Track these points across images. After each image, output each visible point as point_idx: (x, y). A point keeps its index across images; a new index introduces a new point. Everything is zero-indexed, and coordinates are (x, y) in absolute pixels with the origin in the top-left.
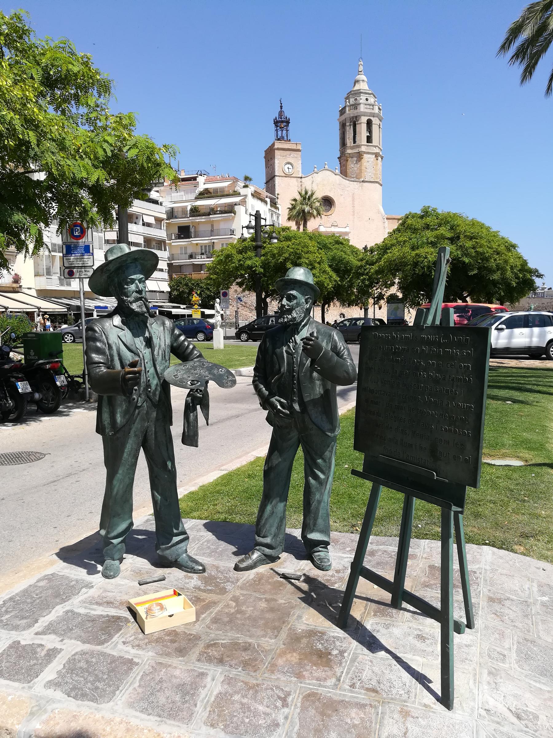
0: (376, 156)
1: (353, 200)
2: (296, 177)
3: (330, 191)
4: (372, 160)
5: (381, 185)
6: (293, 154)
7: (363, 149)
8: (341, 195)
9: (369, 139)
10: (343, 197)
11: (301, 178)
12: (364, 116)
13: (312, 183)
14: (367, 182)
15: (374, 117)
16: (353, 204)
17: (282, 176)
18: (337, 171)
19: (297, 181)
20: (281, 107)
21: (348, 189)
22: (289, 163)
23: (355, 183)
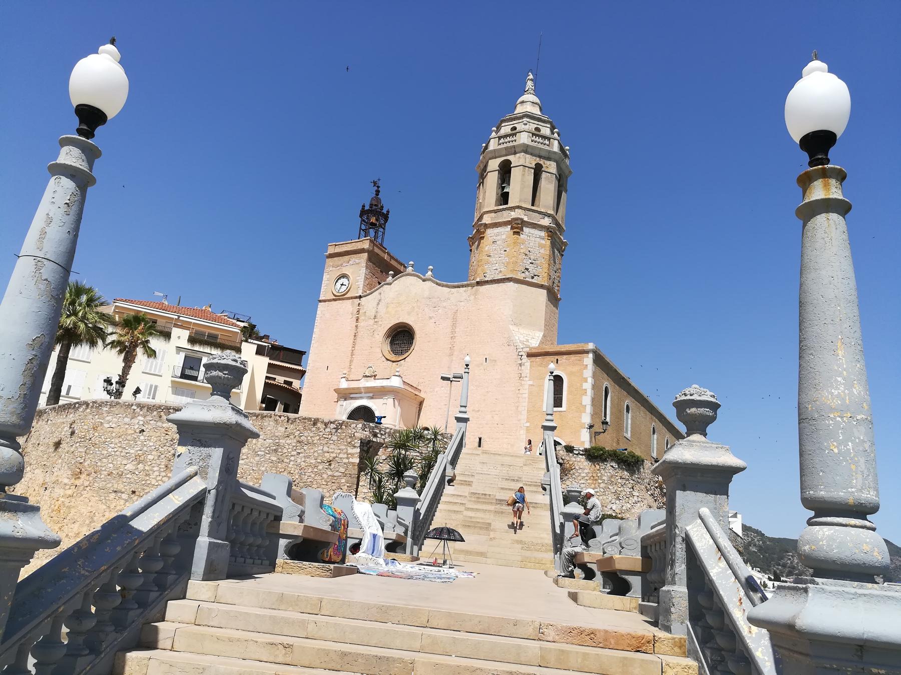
0: (512, 228)
1: (454, 325)
2: (352, 298)
3: (409, 313)
4: (504, 237)
5: (541, 286)
6: (354, 259)
7: (487, 219)
8: (430, 318)
9: (504, 198)
10: (433, 320)
11: (360, 297)
12: (495, 158)
13: (378, 304)
14: (487, 282)
15: (515, 153)
16: (453, 332)
17: (329, 301)
18: (430, 273)
19: (353, 304)
20: (378, 192)
21: (444, 304)
22: (344, 276)
23: (462, 289)
